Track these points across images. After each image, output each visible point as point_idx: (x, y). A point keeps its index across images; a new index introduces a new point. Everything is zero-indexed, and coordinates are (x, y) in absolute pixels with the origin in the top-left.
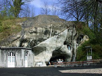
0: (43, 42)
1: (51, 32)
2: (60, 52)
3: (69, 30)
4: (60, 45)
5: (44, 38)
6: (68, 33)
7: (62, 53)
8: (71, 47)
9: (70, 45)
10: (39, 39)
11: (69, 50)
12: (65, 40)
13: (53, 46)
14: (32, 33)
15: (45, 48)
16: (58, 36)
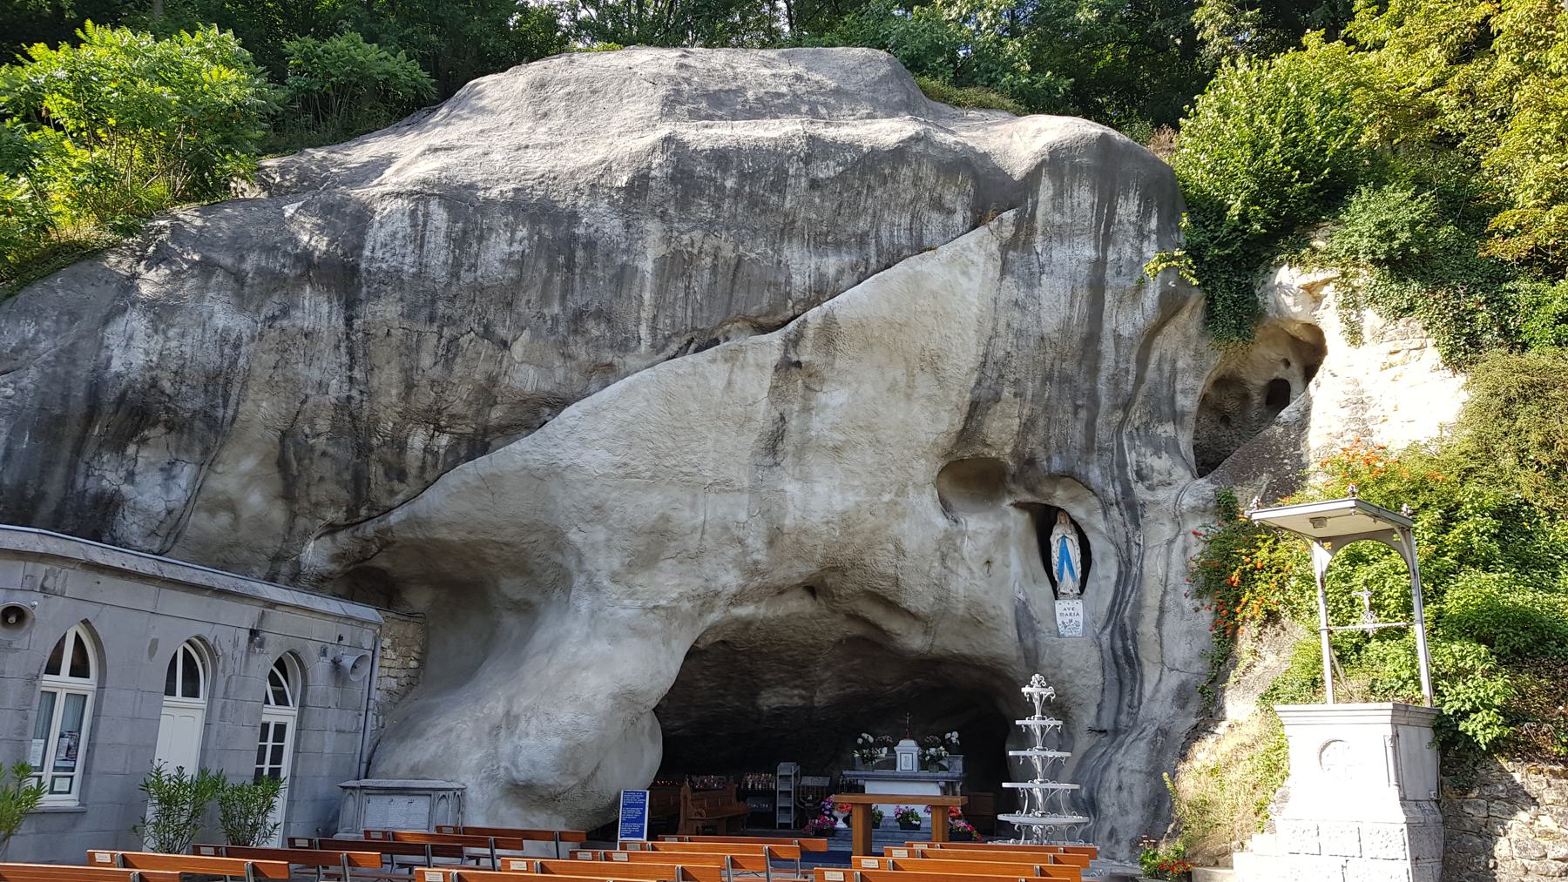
0: (523, 451)
1: (647, 265)
2: (876, 613)
3: (1020, 240)
4: (842, 502)
5: (526, 378)
6: (1012, 289)
7: (916, 641)
8: (1097, 545)
9: (1078, 512)
10: (409, 387)
11: (1068, 583)
12: (949, 421)
13: (685, 517)
14: (273, 281)
15: (557, 540)
16: (794, 342)
